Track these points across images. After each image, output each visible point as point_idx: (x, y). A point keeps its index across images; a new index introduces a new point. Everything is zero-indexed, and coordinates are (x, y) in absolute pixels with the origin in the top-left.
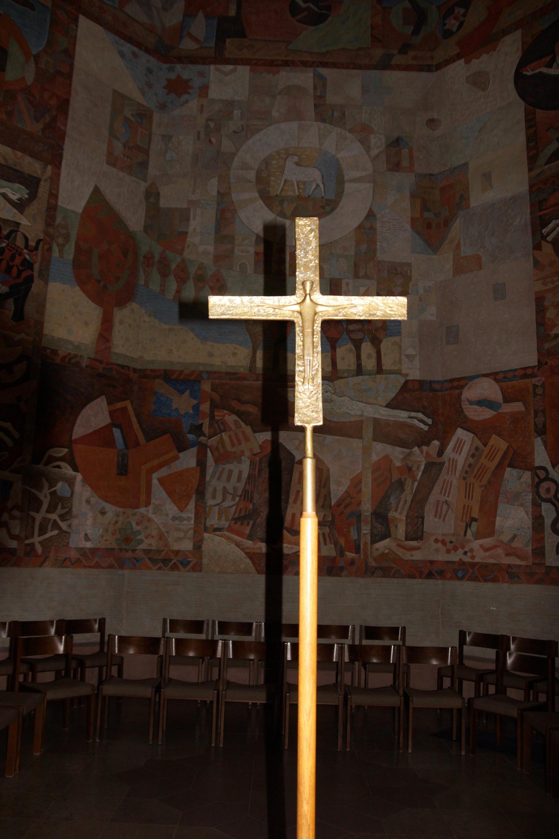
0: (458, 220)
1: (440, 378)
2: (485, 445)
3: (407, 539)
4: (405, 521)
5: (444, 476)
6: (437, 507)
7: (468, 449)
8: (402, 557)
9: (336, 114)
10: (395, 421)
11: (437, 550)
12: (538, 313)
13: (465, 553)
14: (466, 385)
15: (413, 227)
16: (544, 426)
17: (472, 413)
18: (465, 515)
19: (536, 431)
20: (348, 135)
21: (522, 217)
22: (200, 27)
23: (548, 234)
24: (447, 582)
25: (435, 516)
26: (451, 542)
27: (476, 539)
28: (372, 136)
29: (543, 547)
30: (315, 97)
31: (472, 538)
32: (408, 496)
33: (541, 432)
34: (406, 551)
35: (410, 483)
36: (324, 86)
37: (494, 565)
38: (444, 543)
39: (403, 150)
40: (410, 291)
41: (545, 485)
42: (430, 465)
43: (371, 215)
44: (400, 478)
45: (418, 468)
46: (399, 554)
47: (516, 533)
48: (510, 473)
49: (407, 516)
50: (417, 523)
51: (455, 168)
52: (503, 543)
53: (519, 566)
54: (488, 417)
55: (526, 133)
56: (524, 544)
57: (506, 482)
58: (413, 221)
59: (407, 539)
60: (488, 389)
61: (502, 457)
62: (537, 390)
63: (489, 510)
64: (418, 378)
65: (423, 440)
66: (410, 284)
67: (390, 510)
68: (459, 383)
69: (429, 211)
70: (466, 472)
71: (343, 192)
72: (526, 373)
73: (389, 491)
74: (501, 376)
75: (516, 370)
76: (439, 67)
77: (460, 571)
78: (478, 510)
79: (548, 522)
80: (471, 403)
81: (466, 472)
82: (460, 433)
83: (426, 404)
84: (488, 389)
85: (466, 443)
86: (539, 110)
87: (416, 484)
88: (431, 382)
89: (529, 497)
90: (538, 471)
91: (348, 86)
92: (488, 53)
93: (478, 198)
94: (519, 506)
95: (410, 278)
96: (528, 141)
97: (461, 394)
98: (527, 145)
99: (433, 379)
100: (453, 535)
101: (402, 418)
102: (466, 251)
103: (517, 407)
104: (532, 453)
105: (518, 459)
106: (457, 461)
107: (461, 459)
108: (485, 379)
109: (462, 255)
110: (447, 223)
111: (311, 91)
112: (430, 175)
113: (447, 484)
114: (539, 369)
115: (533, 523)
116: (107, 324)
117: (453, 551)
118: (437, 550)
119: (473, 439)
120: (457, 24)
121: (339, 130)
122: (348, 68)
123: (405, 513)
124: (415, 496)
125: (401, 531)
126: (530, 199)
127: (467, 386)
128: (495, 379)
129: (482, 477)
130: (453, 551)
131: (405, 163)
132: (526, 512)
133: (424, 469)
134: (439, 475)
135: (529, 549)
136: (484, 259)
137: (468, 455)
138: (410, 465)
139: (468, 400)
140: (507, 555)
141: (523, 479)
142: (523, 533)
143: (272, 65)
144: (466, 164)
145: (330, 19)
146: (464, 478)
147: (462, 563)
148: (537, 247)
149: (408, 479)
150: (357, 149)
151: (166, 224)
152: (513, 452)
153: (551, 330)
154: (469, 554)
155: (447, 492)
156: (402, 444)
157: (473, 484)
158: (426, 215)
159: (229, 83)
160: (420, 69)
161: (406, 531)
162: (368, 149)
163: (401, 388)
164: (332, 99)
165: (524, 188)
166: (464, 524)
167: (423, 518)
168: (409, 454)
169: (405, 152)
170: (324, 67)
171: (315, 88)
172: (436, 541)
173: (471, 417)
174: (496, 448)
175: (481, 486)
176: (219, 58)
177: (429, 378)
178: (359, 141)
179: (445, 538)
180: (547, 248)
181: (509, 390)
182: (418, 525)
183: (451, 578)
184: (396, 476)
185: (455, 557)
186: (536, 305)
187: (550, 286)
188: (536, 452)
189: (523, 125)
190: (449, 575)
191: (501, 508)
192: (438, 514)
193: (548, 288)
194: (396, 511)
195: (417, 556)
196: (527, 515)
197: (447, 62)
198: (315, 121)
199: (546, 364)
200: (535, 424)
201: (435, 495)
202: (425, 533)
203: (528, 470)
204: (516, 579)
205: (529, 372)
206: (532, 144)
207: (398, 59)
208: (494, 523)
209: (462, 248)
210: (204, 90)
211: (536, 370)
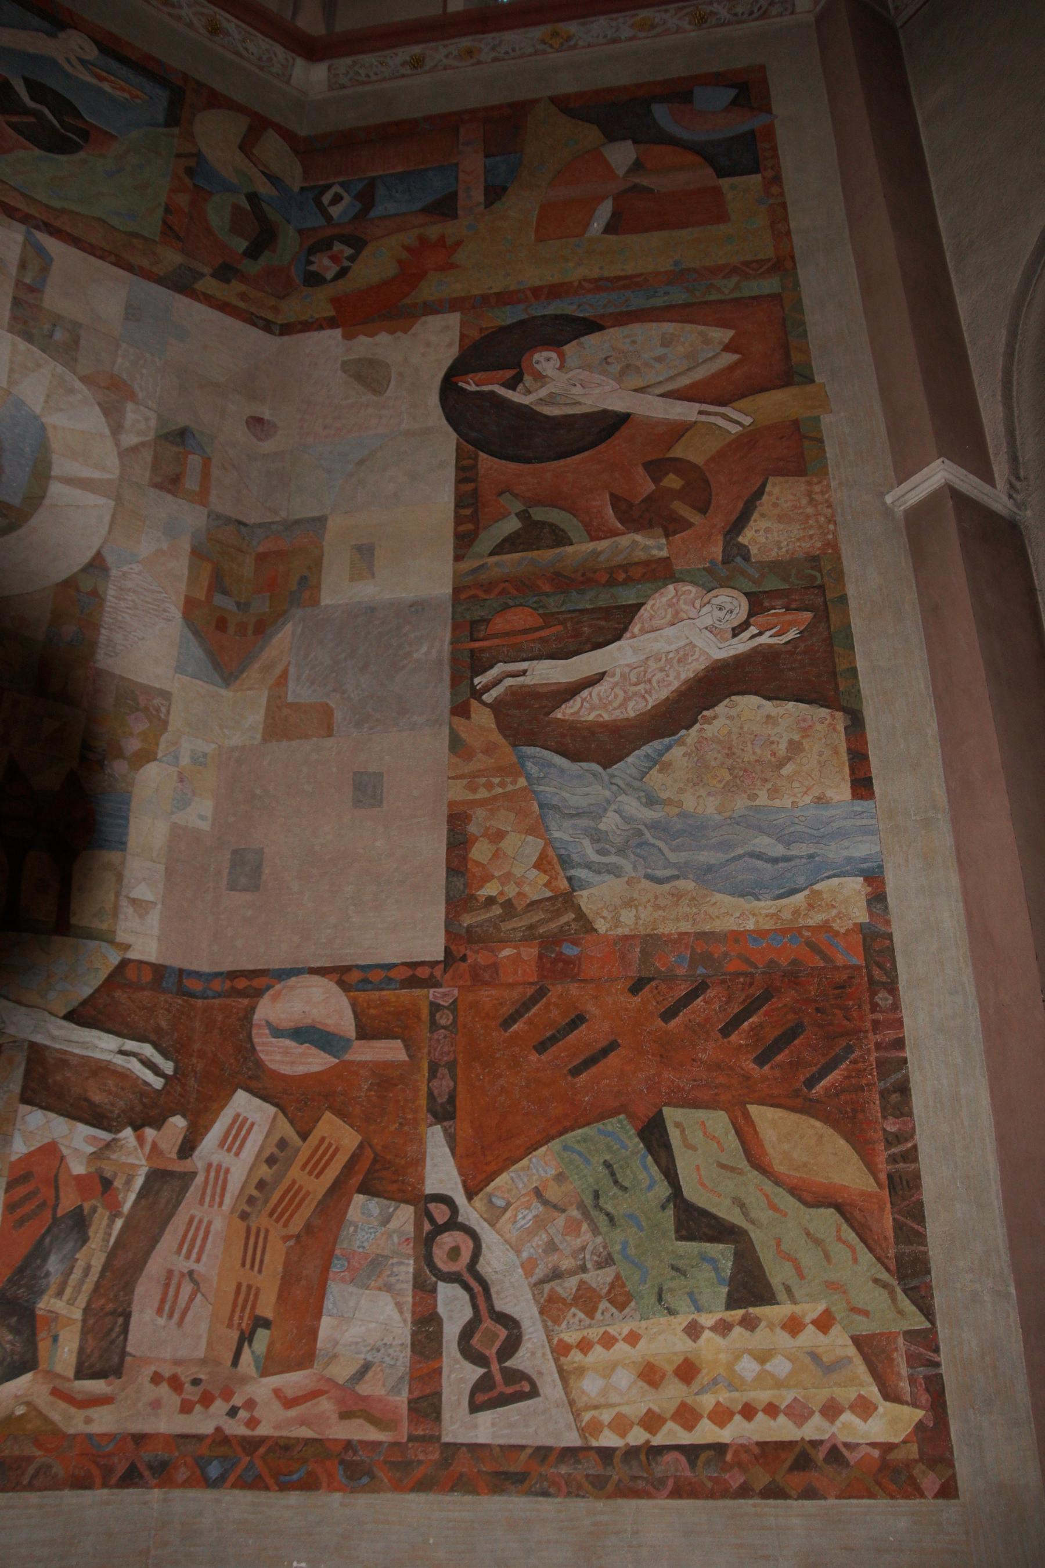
0: (289, 626)
1: (204, 967)
2: (304, 1136)
3: (79, 1375)
4: (79, 1325)
5: (189, 1207)
6: (167, 1286)
7: (260, 1143)
8: (61, 1425)
9: (58, 335)
10: (83, 1057)
11: (156, 1404)
12: (451, 847)
13: (233, 1412)
14: (268, 988)
15: (187, 616)
16: (452, 1098)
17: (278, 1058)
18: (238, 1309)
19: (431, 1111)
20: (78, 385)
21: (435, 645)
23: (487, 689)
24: (177, 1493)
25: (160, 1311)
26: (196, 1382)
27: (264, 1373)
28: (130, 406)
29: (438, 1394)
30: (19, 283)
31: (252, 1371)
32: (94, 1254)
33: (444, 1112)
34: (73, 1410)
35: (105, 1222)
36: (45, 269)
37: (307, 1442)
38: (176, 1384)
39: (191, 457)
40: (160, 755)
41: (448, 1239)
42: (158, 1177)
44: (80, 1207)
45: (129, 1182)
46: (55, 1416)
47: (370, 1358)
48: (362, 1209)
49: (86, 1311)
50: (111, 1330)
51: (297, 522)
52: (336, 1384)
53: (375, 1445)
54: (315, 1068)
55: (457, 489)
56: (386, 1385)
57: (352, 1229)
58: (190, 605)
59: (79, 1375)
60: (324, 1004)
61: (345, 1167)
62: (438, 1016)
63: (303, 1298)
64: (153, 958)
65: (147, 1113)
66: (163, 739)
67: (42, 1292)
68: (250, 984)
69: (225, 592)
70: (251, 1201)
71: (43, 497)
72: (415, 975)
73: (48, 1240)
74: (355, 976)
75: (394, 966)
76: (286, 329)
77: (215, 1463)
78: (273, 1298)
79: (451, 1331)
80: (277, 1032)
81: (251, 1201)
82: (242, 1102)
83: (163, 1024)
84: (324, 1004)
85: (255, 1128)
86: (486, 456)
87: (119, 1223)
88: (181, 971)
89: (406, 1269)
90: (432, 1206)
91: (97, 295)
92: (392, 333)
93: (339, 590)
94: (380, 1289)
95: (165, 724)
96: (460, 503)
97: (253, 1009)
98: (456, 512)
99: (186, 966)
100: (203, 1362)
101: (103, 1050)
102: (298, 692)
103: (390, 1051)
104: (419, 1162)
105: (384, 1173)
106: (227, 1171)
107: (239, 1168)
108: (316, 979)
109: (290, 699)
110: (263, 628)
111: (13, 270)
112: (240, 523)
113: (198, 1229)
114: (445, 971)
115: (414, 1334)
117: (198, 1408)
118: (156, 1404)
119: (275, 1118)
120: (335, 269)
121: (60, 369)
122: (101, 258)
123: (82, 1301)
124: (112, 1255)
125: (64, 1352)
126: (454, 613)
127: (271, 992)
128: (342, 984)
129: (291, 1216)
130: (198, 1408)
131: (191, 483)
132: (399, 1306)
133: (143, 1188)
134: (179, 1203)
135: (402, 1399)
136: (338, 716)
137: (258, 1156)
138: (108, 1175)
139: (268, 1024)
140: (345, 1415)
141: (393, 1225)
142: (387, 1359)
144: (321, 521)
145: (82, 155)
146: (244, 1216)
147: (221, 1438)
148: (461, 710)
149: (100, 1210)
150: (93, 420)
152: (372, 1156)
153: (481, 887)
154: (243, 1414)
155: (196, 1250)
156: (97, 1118)
157: (267, 1231)
158: (219, 600)
160: (251, 319)
161: (81, 1350)
162: (117, 429)
163: (111, 976)
164: (55, 300)
165: (446, 590)
166: (235, 1335)
167: (127, 1316)
168: (108, 1146)
169: (194, 461)
170: (51, 234)
171: (23, 265)
172: (156, 1379)
173: (272, 1066)
174: (330, 1145)
175: (286, 1238)
177: (176, 961)
178: (99, 404)
179: (179, 1370)
180: (483, 718)
181: (373, 1011)
182: (114, 1335)
183: (187, 1484)
184: (68, 1202)
185: (203, 1423)
186: (450, 831)
187: (482, 794)
188: (428, 1159)
189: (450, 473)
190: (182, 1474)
191: (335, 1291)
192: (167, 1307)
193: (477, 797)
194: (60, 1294)
195: (103, 1422)
196: (401, 1312)
197: (307, 326)
198: (10, 331)
199: (464, 958)
200: (431, 1095)
201: (165, 1257)
202: (128, 1359)
203: (407, 1202)
204: (365, 1480)
205: (423, 973)
206: (467, 512)
207: (208, 284)
208: (314, 1333)
209: (291, 685)
211: (438, 971)
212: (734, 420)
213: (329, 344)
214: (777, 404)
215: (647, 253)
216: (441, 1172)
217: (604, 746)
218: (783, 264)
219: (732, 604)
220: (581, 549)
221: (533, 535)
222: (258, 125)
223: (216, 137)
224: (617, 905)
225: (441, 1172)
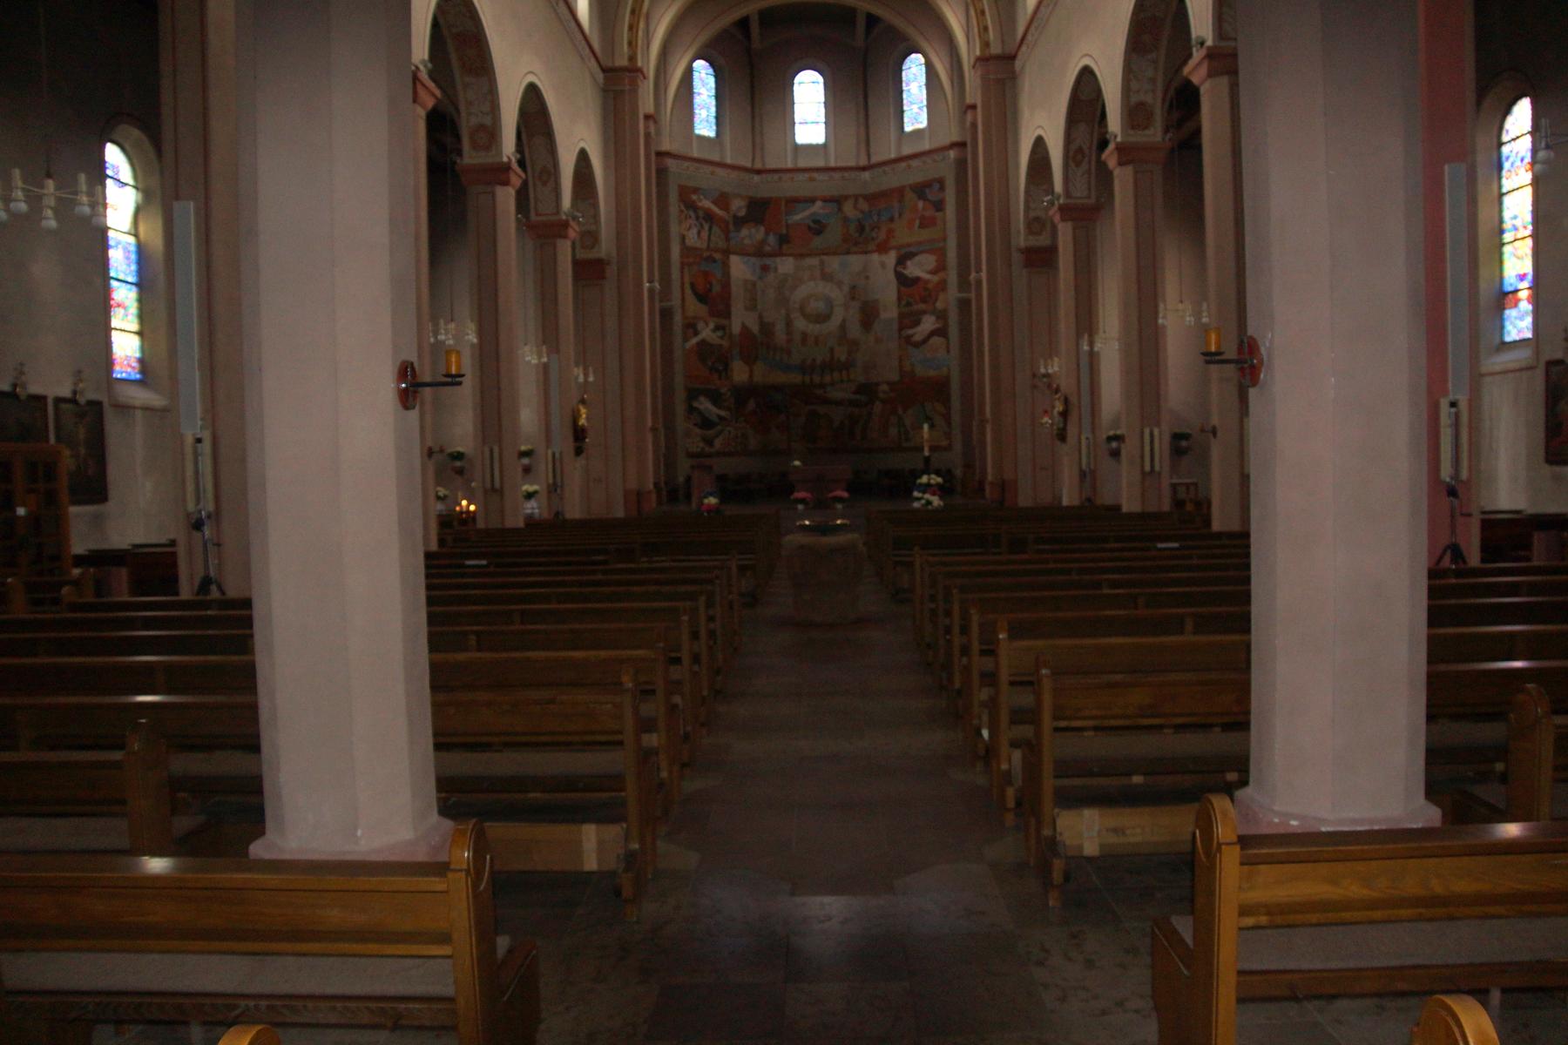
21: (895, 326)
22: (772, 239)
43: (844, 320)
60: (885, 387)
91: (834, 263)
93: (884, 315)
116: (751, 371)
143: (802, 256)
151: (767, 329)
159: (786, 265)
176: (781, 255)
210: (776, 269)
212: (935, 279)
213: (875, 257)
214: (941, 275)
215: (925, 234)
216: (900, 411)
217: (917, 345)
218: (944, 239)
219: (933, 318)
220: (915, 307)
221: (909, 304)
222: (856, 197)
223: (848, 209)
224: (920, 371)
225: (900, 411)
